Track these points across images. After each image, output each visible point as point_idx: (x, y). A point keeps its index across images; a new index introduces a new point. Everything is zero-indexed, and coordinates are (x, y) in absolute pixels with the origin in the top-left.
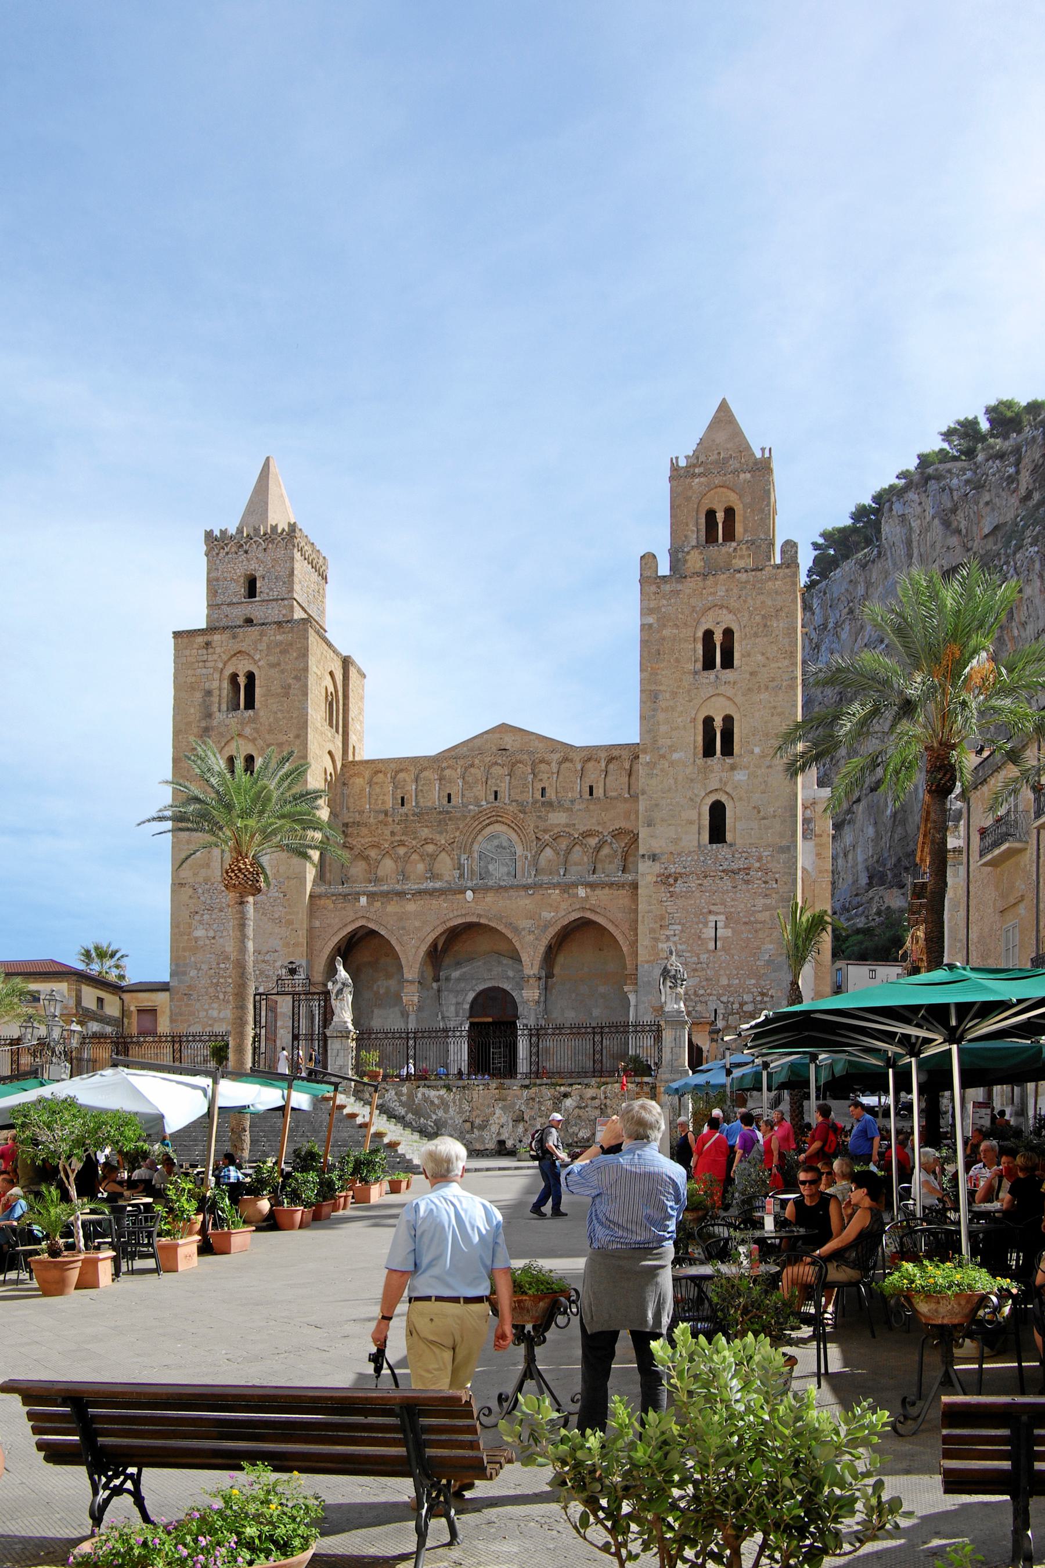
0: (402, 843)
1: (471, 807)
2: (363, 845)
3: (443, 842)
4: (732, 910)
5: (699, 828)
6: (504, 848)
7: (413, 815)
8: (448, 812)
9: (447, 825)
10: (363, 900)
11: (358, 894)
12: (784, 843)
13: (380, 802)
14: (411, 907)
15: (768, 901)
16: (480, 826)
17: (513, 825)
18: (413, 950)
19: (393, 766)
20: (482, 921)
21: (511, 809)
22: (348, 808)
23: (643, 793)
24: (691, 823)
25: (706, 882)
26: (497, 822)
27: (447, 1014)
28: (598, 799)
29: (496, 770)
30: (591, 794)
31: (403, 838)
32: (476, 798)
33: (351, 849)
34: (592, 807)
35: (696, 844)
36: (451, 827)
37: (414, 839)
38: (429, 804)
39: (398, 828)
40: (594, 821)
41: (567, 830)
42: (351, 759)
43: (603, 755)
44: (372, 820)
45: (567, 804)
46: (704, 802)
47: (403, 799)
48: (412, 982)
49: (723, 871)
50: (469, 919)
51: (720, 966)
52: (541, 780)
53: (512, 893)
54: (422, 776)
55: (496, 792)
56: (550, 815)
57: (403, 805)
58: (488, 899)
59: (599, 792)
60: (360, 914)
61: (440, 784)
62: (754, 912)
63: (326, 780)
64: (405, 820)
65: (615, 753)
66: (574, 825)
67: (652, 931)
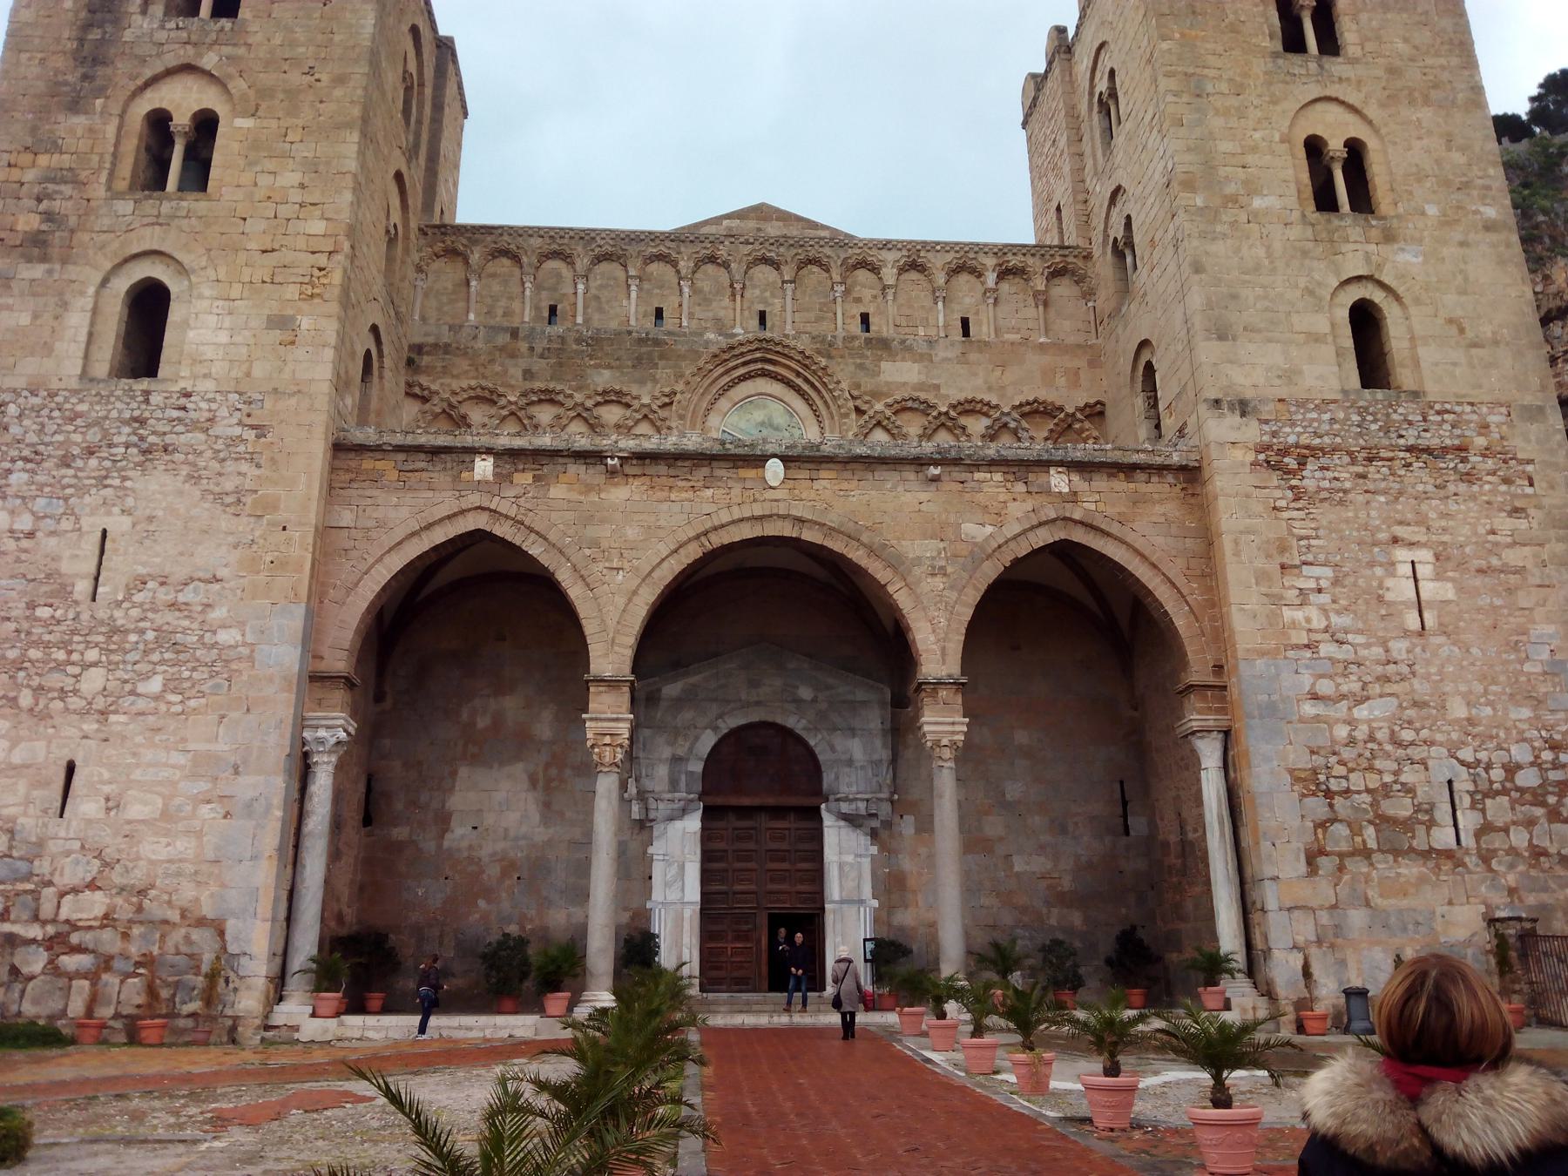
1: (711, 336)
2: (454, 393)
3: (646, 400)
4: (1446, 538)
5: (1338, 355)
6: (777, 429)
7: (579, 341)
8: (657, 342)
9: (656, 366)
11: (473, 451)
12: (1528, 399)
13: (500, 312)
15: (1522, 524)
16: (726, 379)
17: (799, 381)
18: (621, 601)
19: (536, 242)
20: (809, 535)
21: (800, 347)
22: (423, 319)
23: (1198, 268)
24: (1317, 338)
25: (1376, 471)
26: (764, 374)
27: (648, 784)
28: (986, 344)
29: (764, 273)
30: (966, 331)
31: (551, 386)
32: (717, 320)
33: (425, 400)
34: (973, 356)
35: (1335, 384)
36: (664, 373)
37: (579, 389)
38: (614, 325)
39: (539, 365)
40: (980, 381)
41: (923, 396)
42: (437, 221)
43: (990, 262)
44: (479, 344)
45: (922, 347)
46: (1338, 300)
47: (553, 310)
48: (612, 684)
49: (1409, 449)
50: (771, 529)
51: (1440, 673)
52: (858, 300)
53: (881, 474)
55: (762, 316)
56: (884, 365)
58: (816, 485)
59: (980, 330)
60: (474, 499)
61: (640, 288)
62: (1497, 544)
64: (558, 354)
65: (1014, 261)
66: (937, 387)
67: (1262, 577)
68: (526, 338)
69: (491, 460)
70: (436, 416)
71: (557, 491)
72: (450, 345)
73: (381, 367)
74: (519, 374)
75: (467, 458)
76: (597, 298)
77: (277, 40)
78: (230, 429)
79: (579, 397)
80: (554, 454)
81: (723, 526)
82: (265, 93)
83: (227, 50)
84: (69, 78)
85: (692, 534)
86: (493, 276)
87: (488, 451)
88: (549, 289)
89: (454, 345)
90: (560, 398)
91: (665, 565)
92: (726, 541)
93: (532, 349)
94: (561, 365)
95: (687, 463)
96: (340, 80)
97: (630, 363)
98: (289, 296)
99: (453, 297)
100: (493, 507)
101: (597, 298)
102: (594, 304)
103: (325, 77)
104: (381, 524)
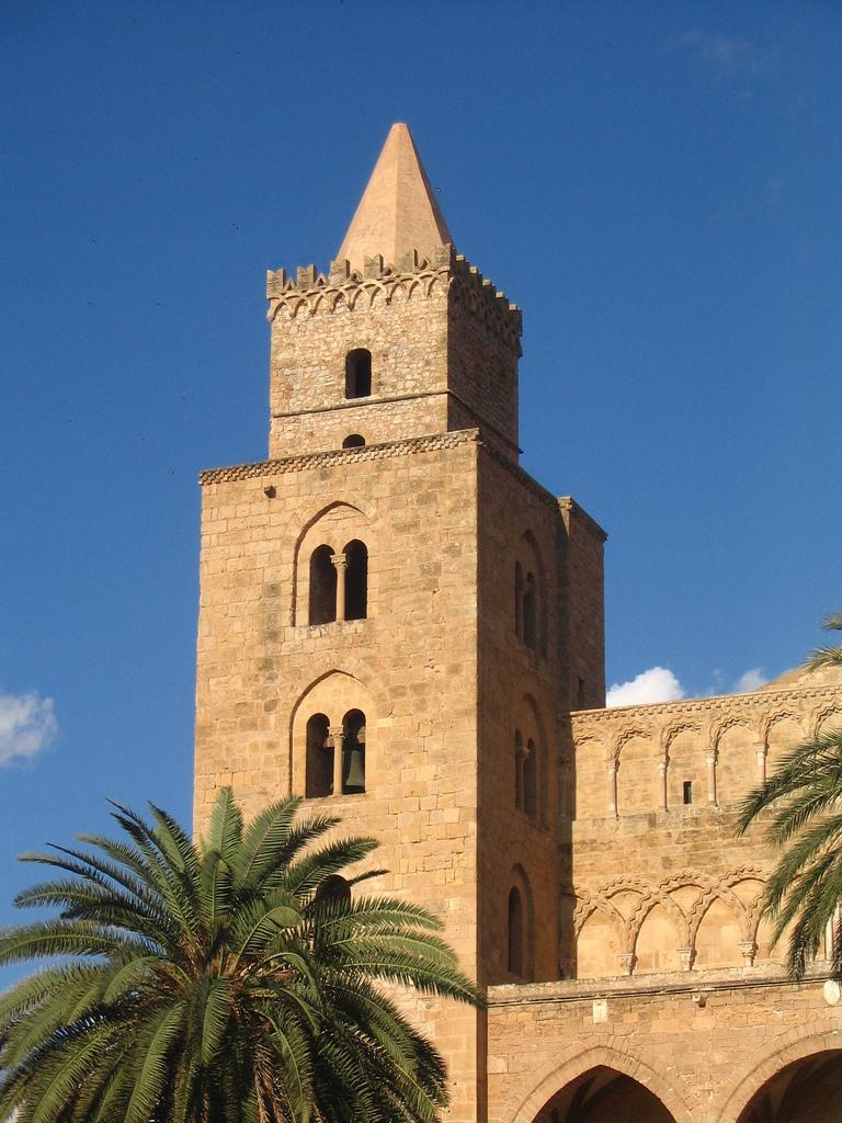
0: (686, 883)
7: (714, 819)
10: (600, 1010)
11: (589, 996)
13: (638, 796)
14: (703, 1022)
19: (665, 718)
31: (690, 870)
44: (621, 835)
47: (687, 785)
54: (724, 737)
57: (687, 800)
63: (518, 755)
68: (664, 823)
69: (604, 1002)
70: (591, 913)
71: (658, 1026)
72: (595, 841)
73: (529, 893)
74: (658, 861)
75: (586, 1003)
76: (727, 768)
77: (401, 637)
78: (408, 1003)
79: (714, 879)
80: (654, 992)
81: (792, 1045)
82: (397, 692)
83: (364, 651)
84: (249, 699)
85: (767, 1055)
86: (629, 757)
87: (603, 996)
88: (682, 765)
89: (599, 841)
90: (697, 882)
91: (747, 1082)
92: (795, 1058)
93: (669, 835)
94: (696, 848)
95: (761, 990)
96: (455, 670)
97: (760, 838)
98: (437, 882)
99: (596, 786)
100: (609, 1045)
101: (727, 768)
102: (725, 776)
103: (442, 668)
104: (527, 1068)
